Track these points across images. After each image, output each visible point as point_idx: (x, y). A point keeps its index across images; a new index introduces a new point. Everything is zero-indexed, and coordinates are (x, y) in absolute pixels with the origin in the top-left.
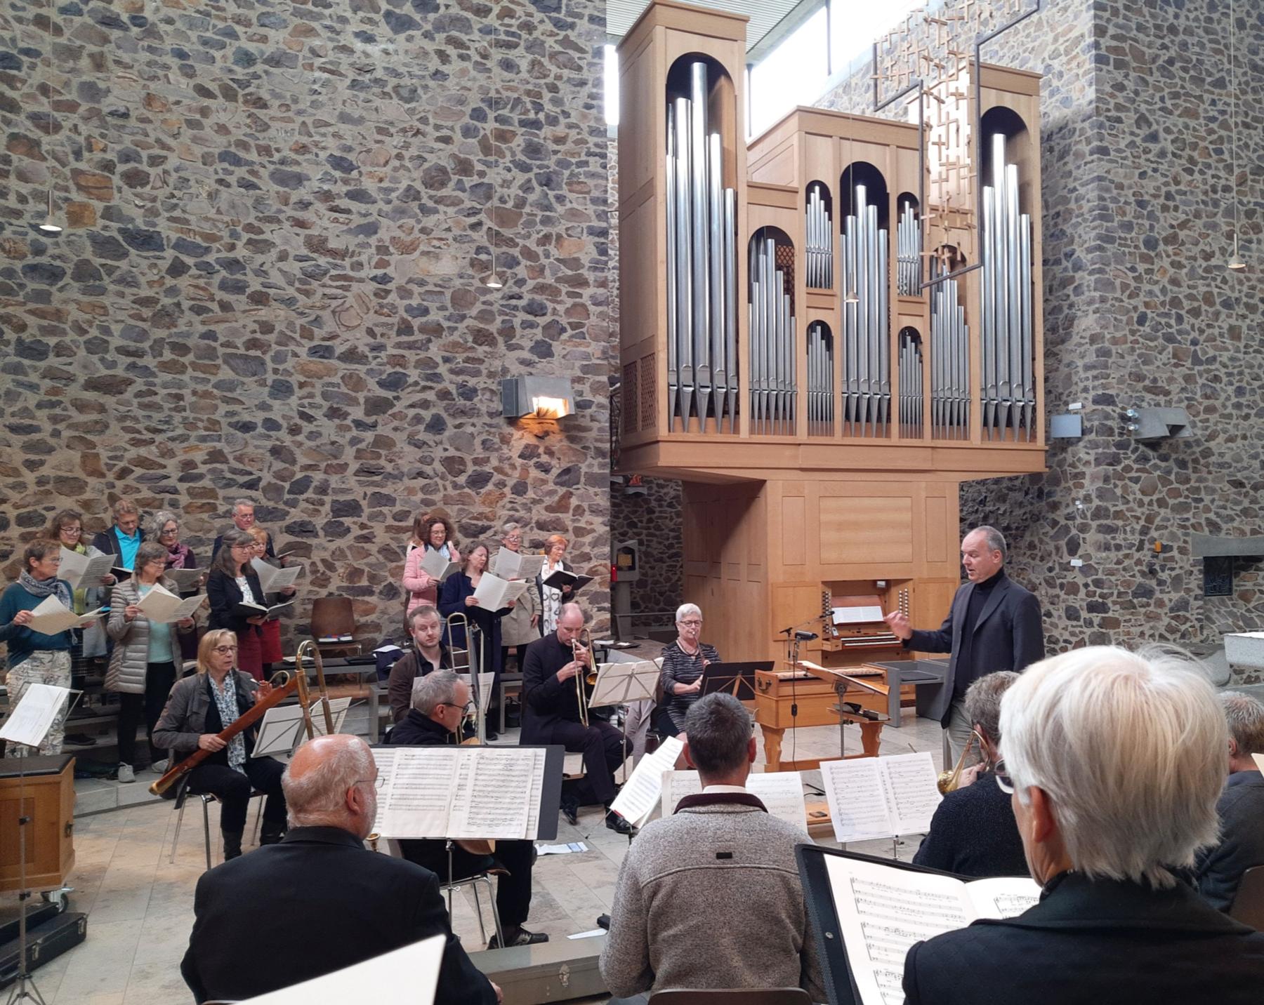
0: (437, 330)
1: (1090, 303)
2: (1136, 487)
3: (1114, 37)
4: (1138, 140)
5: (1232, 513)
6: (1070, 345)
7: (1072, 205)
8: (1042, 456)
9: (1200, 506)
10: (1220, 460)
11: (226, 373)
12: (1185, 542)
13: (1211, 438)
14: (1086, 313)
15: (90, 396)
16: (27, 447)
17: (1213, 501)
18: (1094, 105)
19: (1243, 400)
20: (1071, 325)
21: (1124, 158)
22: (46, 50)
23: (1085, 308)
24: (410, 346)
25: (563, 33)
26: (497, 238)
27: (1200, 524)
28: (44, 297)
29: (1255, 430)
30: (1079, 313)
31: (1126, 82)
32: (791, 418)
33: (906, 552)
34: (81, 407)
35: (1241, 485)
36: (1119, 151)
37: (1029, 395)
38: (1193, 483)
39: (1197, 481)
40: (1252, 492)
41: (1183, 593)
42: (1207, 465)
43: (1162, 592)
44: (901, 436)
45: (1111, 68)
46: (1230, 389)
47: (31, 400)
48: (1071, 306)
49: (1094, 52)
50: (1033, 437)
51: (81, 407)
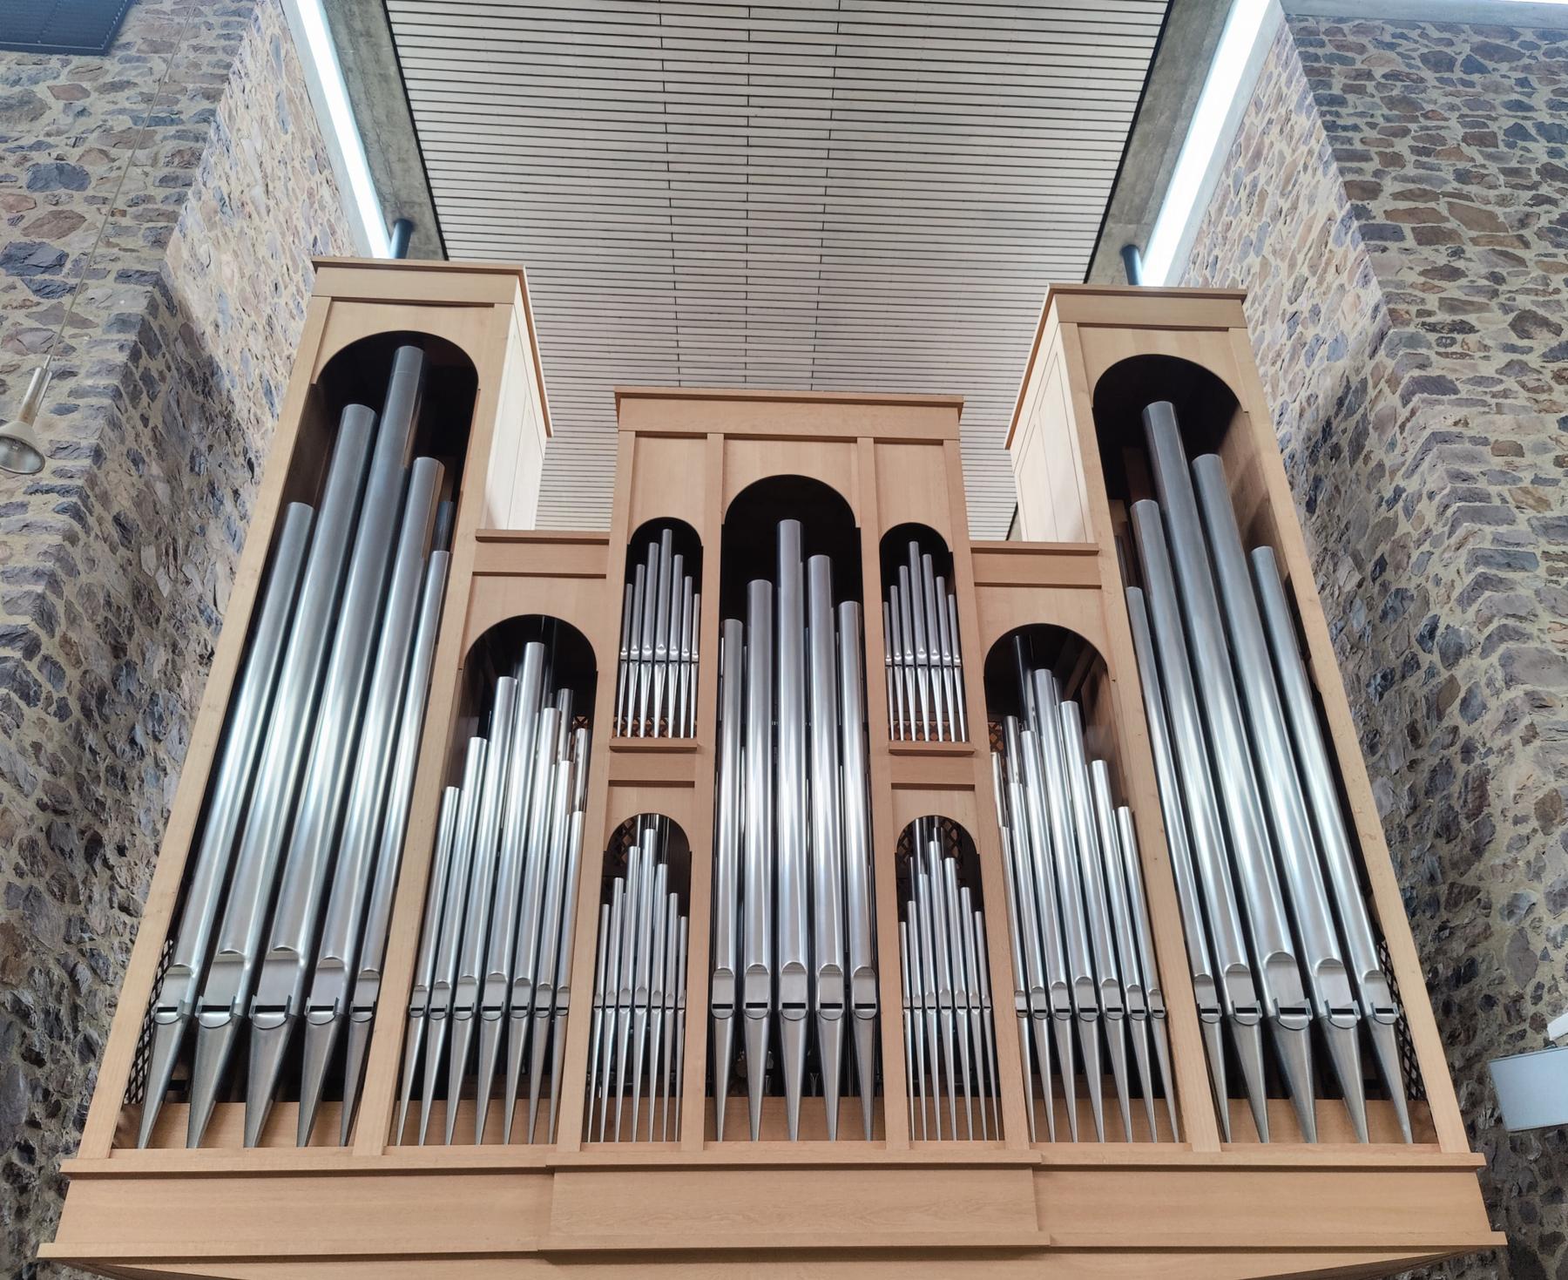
1: (1509, 721)
3: (1396, 196)
4: (1533, 360)
6: (1495, 856)
7: (1404, 527)
8: (1470, 1193)
14: (1506, 752)
18: (1384, 309)
20: (1483, 799)
21: (1505, 394)
23: (1499, 742)
25: (47, 303)
30: (1492, 761)
31: (1460, 264)
32: (545, 1092)
36: (1480, 381)
37: (1375, 995)
44: (916, 1134)
45: (1410, 242)
48: (1468, 751)
49: (1356, 224)
50: (1425, 1129)
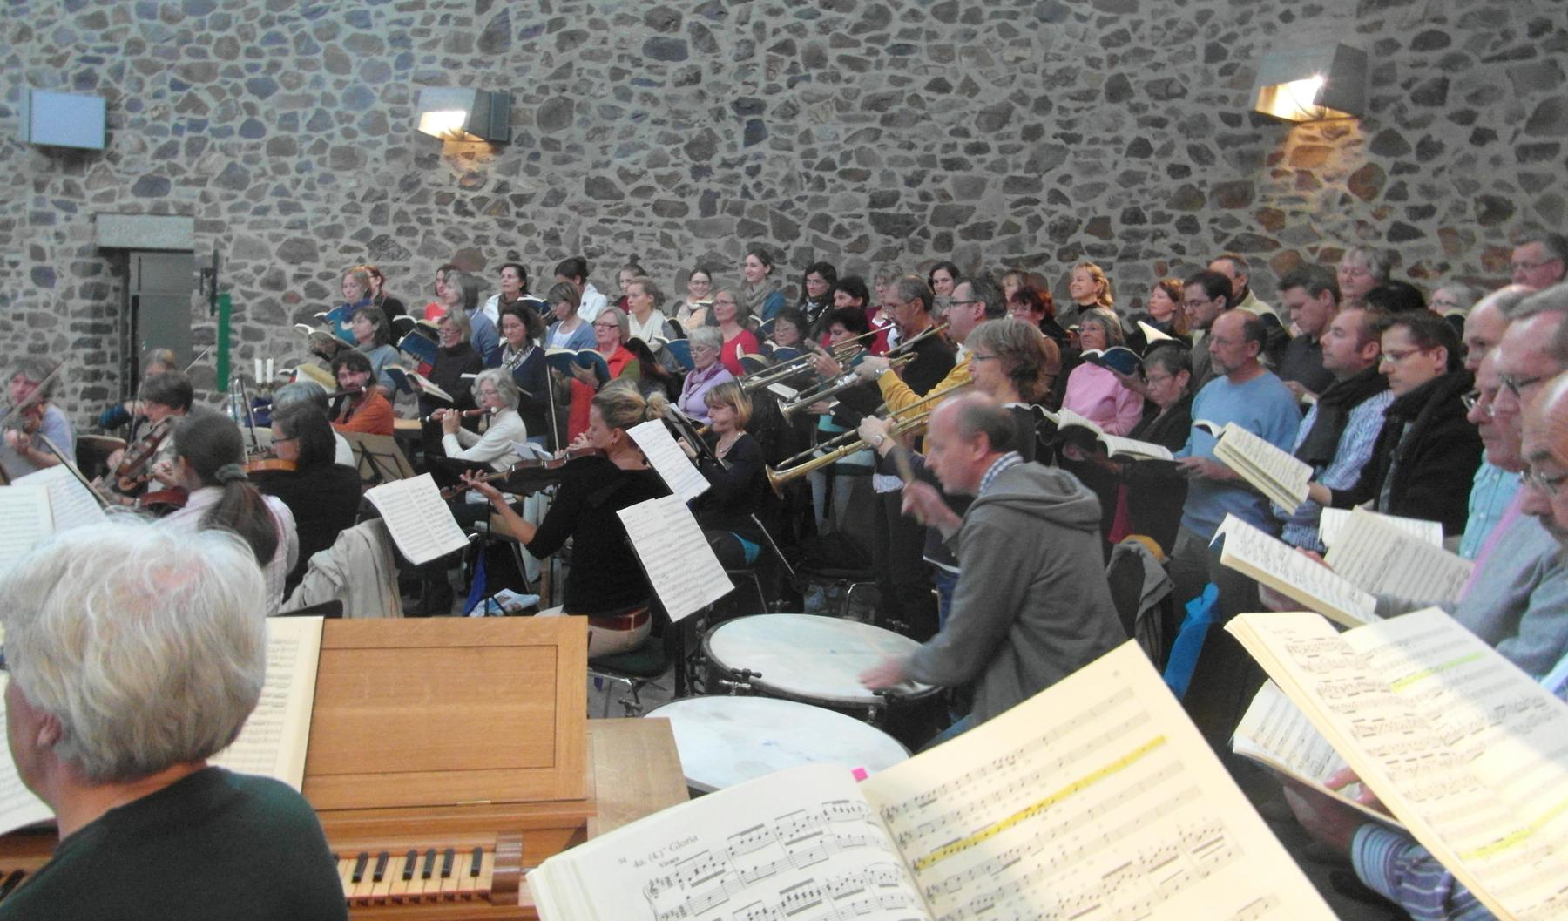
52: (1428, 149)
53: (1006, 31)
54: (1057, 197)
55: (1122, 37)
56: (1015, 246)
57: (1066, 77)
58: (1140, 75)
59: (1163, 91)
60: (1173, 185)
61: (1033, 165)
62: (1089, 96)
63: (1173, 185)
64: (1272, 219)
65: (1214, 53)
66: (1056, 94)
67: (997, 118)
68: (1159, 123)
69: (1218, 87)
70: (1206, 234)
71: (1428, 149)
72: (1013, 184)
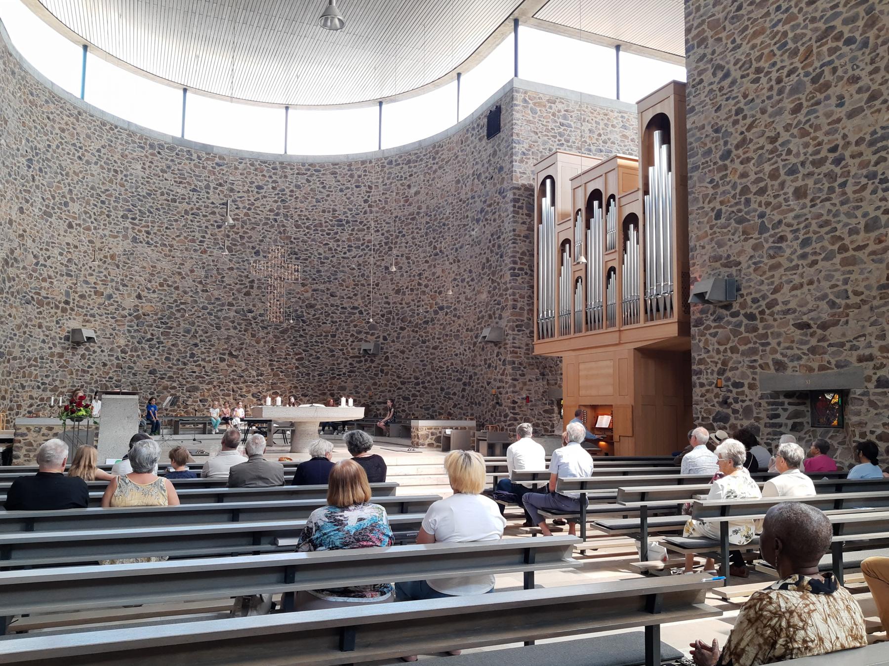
0: (483, 317)
2: (714, 340)
5: (799, 352)
9: (768, 348)
10: (784, 308)
11: (454, 340)
12: (754, 379)
13: (776, 291)
15: (433, 351)
16: (424, 365)
17: (779, 344)
19: (808, 250)
22: (426, 268)
24: (479, 324)
26: (493, 281)
27: (767, 364)
28: (425, 328)
29: (823, 274)
33: (610, 390)
34: (431, 354)
35: (808, 326)
38: (761, 331)
39: (764, 329)
40: (819, 332)
41: (753, 421)
42: (772, 314)
43: (736, 419)
46: (796, 244)
47: (424, 353)
51: (431, 354)
52: (94, 352)
53: (21, 304)
54: (28, 351)
55: (40, 313)
56: (21, 364)
57: (30, 320)
58: (45, 324)
59: (48, 328)
60: (49, 351)
61: (24, 342)
62: (34, 326)
63: (49, 351)
64: (67, 361)
65: (57, 323)
66: (29, 323)
67: (19, 327)
68: (47, 336)
69: (58, 330)
70: (55, 363)
71: (94, 352)
72: (21, 346)
